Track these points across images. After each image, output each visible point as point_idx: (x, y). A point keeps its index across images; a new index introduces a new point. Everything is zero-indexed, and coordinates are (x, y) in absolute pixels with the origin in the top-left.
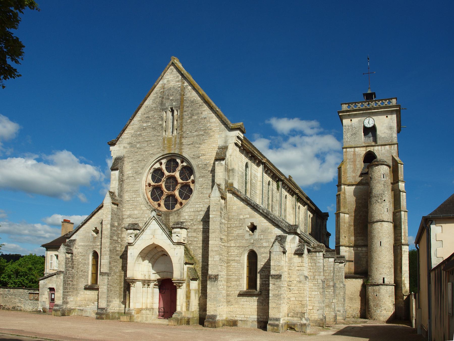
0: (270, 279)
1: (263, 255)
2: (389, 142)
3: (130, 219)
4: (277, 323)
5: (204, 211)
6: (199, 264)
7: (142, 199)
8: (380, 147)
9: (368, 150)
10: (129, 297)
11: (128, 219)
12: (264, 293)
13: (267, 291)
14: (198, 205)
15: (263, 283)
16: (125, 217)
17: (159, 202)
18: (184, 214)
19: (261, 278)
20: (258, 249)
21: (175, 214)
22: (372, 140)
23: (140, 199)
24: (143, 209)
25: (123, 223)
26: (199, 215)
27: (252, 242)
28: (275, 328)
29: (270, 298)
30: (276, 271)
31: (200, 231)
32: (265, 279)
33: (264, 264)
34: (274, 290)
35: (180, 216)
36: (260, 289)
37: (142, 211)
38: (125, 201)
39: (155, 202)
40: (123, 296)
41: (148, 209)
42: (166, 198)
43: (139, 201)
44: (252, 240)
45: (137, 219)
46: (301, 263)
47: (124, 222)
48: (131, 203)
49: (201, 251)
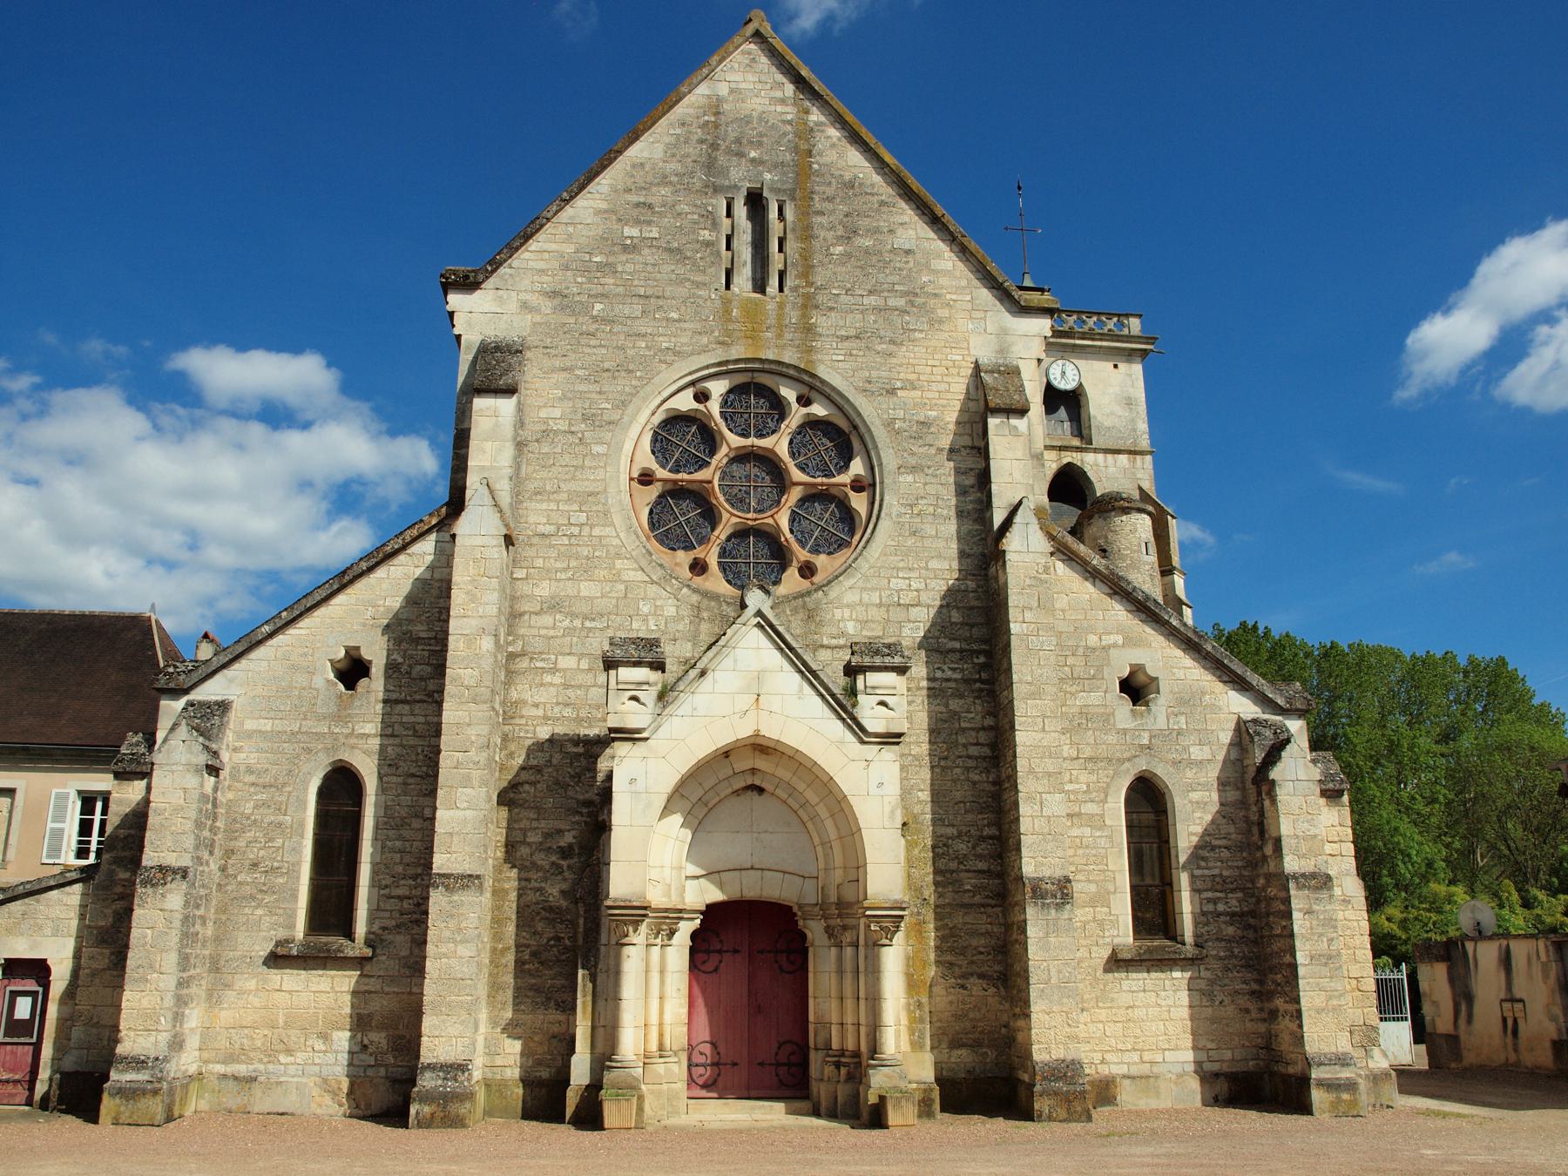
0: (1292, 892)
1: (1195, 796)
2: (1128, 444)
3: (558, 617)
4: (1345, 1074)
5: (929, 606)
6: (918, 831)
7: (622, 535)
8: (1100, 456)
9: (1065, 461)
10: (589, 998)
11: (547, 620)
12: (1214, 952)
13: (1223, 944)
14: (900, 581)
15: (1205, 909)
16: (526, 609)
17: (699, 552)
18: (838, 614)
19: (1195, 890)
20: (1171, 769)
21: (795, 611)
22: (1068, 432)
23: (608, 531)
24: (627, 578)
25: (517, 637)
26: (909, 621)
27: (1146, 742)
28: (1345, 1096)
29: (1301, 971)
30: (1304, 856)
31: (919, 689)
32: (1210, 895)
33: (1199, 829)
34: (1313, 934)
35: (818, 619)
36: (1196, 936)
37: (622, 587)
38: (529, 537)
39: (681, 554)
40: (510, 993)
41: (655, 578)
42: (729, 539)
43: (604, 542)
44: (1146, 735)
45: (593, 620)
46: (1338, 828)
47: (522, 631)
48: (562, 549)
49: (926, 774)
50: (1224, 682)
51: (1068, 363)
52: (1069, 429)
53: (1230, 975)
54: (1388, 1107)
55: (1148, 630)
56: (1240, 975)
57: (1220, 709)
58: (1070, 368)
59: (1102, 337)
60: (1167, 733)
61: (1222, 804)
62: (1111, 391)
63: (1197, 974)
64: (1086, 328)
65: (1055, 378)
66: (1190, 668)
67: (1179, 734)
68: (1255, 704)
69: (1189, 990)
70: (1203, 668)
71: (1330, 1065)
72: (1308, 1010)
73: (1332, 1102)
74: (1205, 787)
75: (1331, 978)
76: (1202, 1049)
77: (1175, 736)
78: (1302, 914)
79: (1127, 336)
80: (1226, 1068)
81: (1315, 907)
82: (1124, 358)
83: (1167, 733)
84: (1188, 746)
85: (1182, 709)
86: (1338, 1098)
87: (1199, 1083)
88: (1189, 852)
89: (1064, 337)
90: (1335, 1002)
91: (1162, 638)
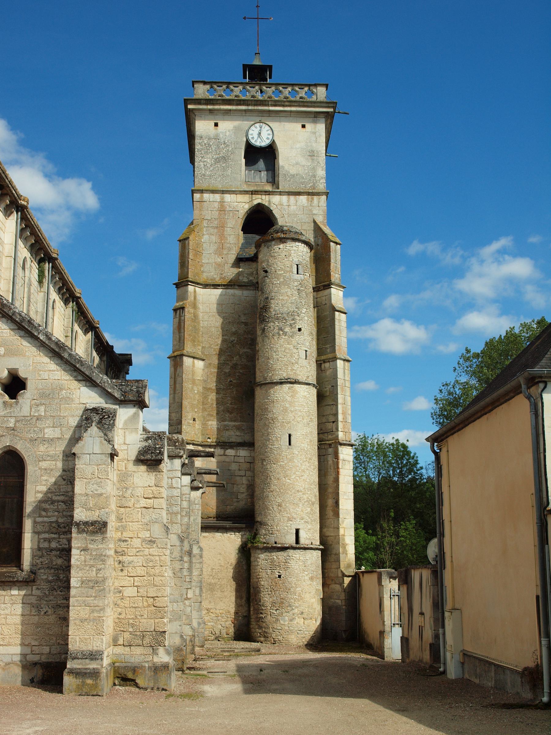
0: (74, 535)
1: (44, 465)
2: (308, 187)
4: (93, 665)
8: (285, 198)
9: (256, 202)
12: (45, 577)
13: (52, 571)
15: (41, 546)
19: (35, 532)
20: (28, 445)
22: (264, 180)
27: (11, 425)
28: (89, 681)
29: (73, 592)
30: (90, 509)
32: (46, 536)
33: (44, 489)
34: (86, 565)
36: (32, 565)
44: (13, 420)
46: (154, 488)
50: (79, 381)
51: (264, 125)
52: (265, 177)
53: (55, 594)
54: (163, 689)
55: (25, 343)
56: (63, 593)
57: (73, 401)
58: (265, 128)
59: (292, 103)
60: (29, 418)
61: (64, 470)
62: (298, 145)
63: (30, 592)
64: (282, 97)
65: (253, 138)
66: (53, 371)
67: (38, 419)
68: (101, 396)
69: (23, 603)
70: (64, 370)
71: (82, 659)
72: (75, 619)
73: (78, 685)
74: (53, 458)
75: (95, 597)
76: (27, 645)
77: (35, 420)
78: (79, 551)
79: (314, 102)
80: (44, 659)
81: (91, 546)
82: (311, 119)
83: (29, 418)
84: (44, 428)
85: (43, 401)
86: (84, 684)
87: (21, 669)
88: (34, 505)
89: (260, 105)
90: (96, 614)
91: (35, 349)
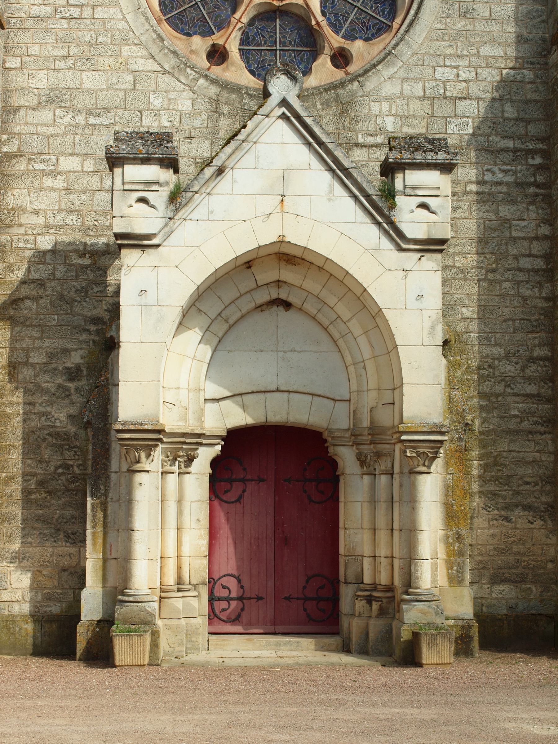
3: (58, 112)
5: (479, 99)
6: (462, 352)
7: (129, 17)
10: (100, 529)
11: (46, 115)
14: (446, 70)
16: (22, 103)
17: (218, 38)
18: (375, 108)
21: (326, 104)
23: (113, 12)
24: (134, 67)
25: (12, 136)
26: (456, 116)
31: (466, 193)
35: (353, 114)
37: (130, 78)
38: (22, 20)
39: (197, 40)
40: (18, 524)
41: (167, 67)
42: (251, 22)
43: (108, 26)
45: (98, 115)
47: (17, 129)
48: (61, 33)
49: (472, 289)
